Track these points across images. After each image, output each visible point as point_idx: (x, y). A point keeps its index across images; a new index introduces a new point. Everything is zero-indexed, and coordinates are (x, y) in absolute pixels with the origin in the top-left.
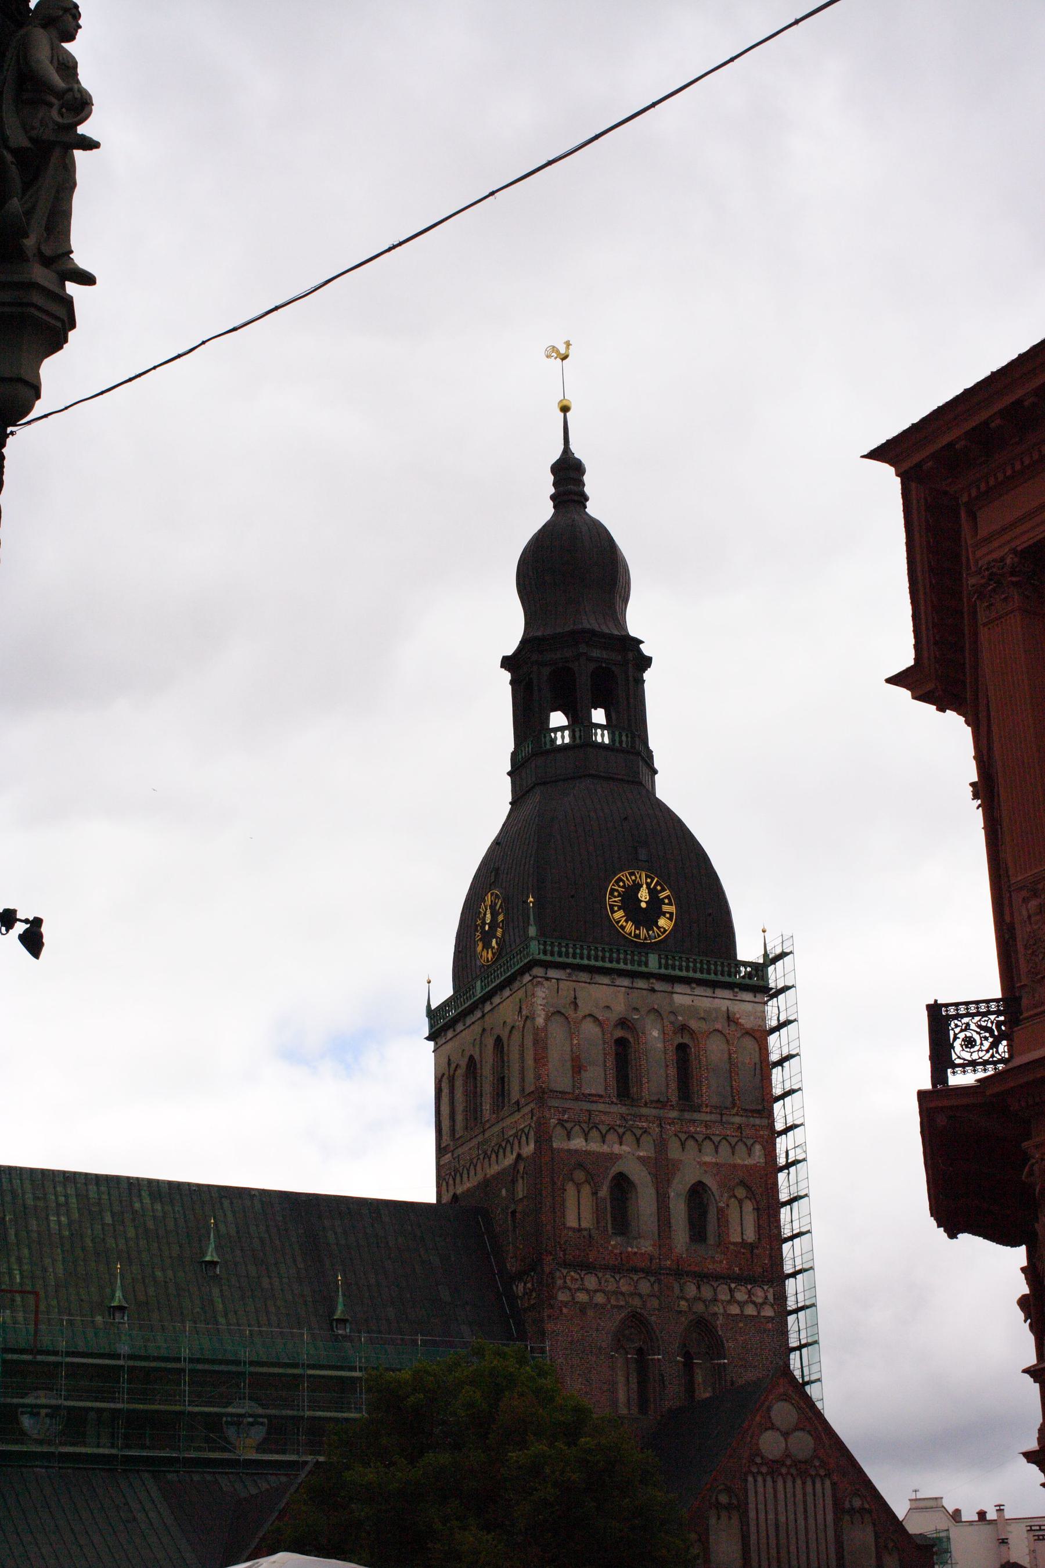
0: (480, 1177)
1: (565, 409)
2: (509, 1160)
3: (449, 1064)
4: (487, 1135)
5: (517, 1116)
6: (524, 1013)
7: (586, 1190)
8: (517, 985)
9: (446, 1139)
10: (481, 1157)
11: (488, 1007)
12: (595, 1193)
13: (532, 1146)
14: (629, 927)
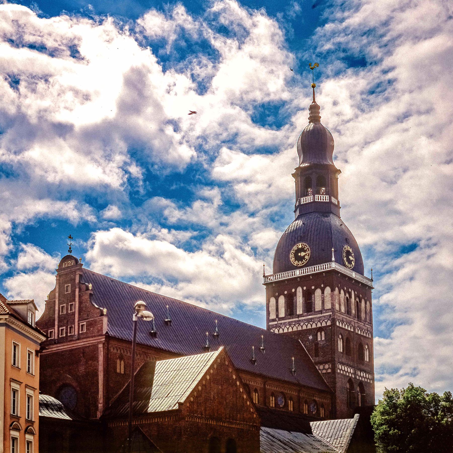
5: (320, 315)
7: (341, 340)
9: (273, 316)
10: (297, 325)
12: (343, 342)
14: (347, 263)
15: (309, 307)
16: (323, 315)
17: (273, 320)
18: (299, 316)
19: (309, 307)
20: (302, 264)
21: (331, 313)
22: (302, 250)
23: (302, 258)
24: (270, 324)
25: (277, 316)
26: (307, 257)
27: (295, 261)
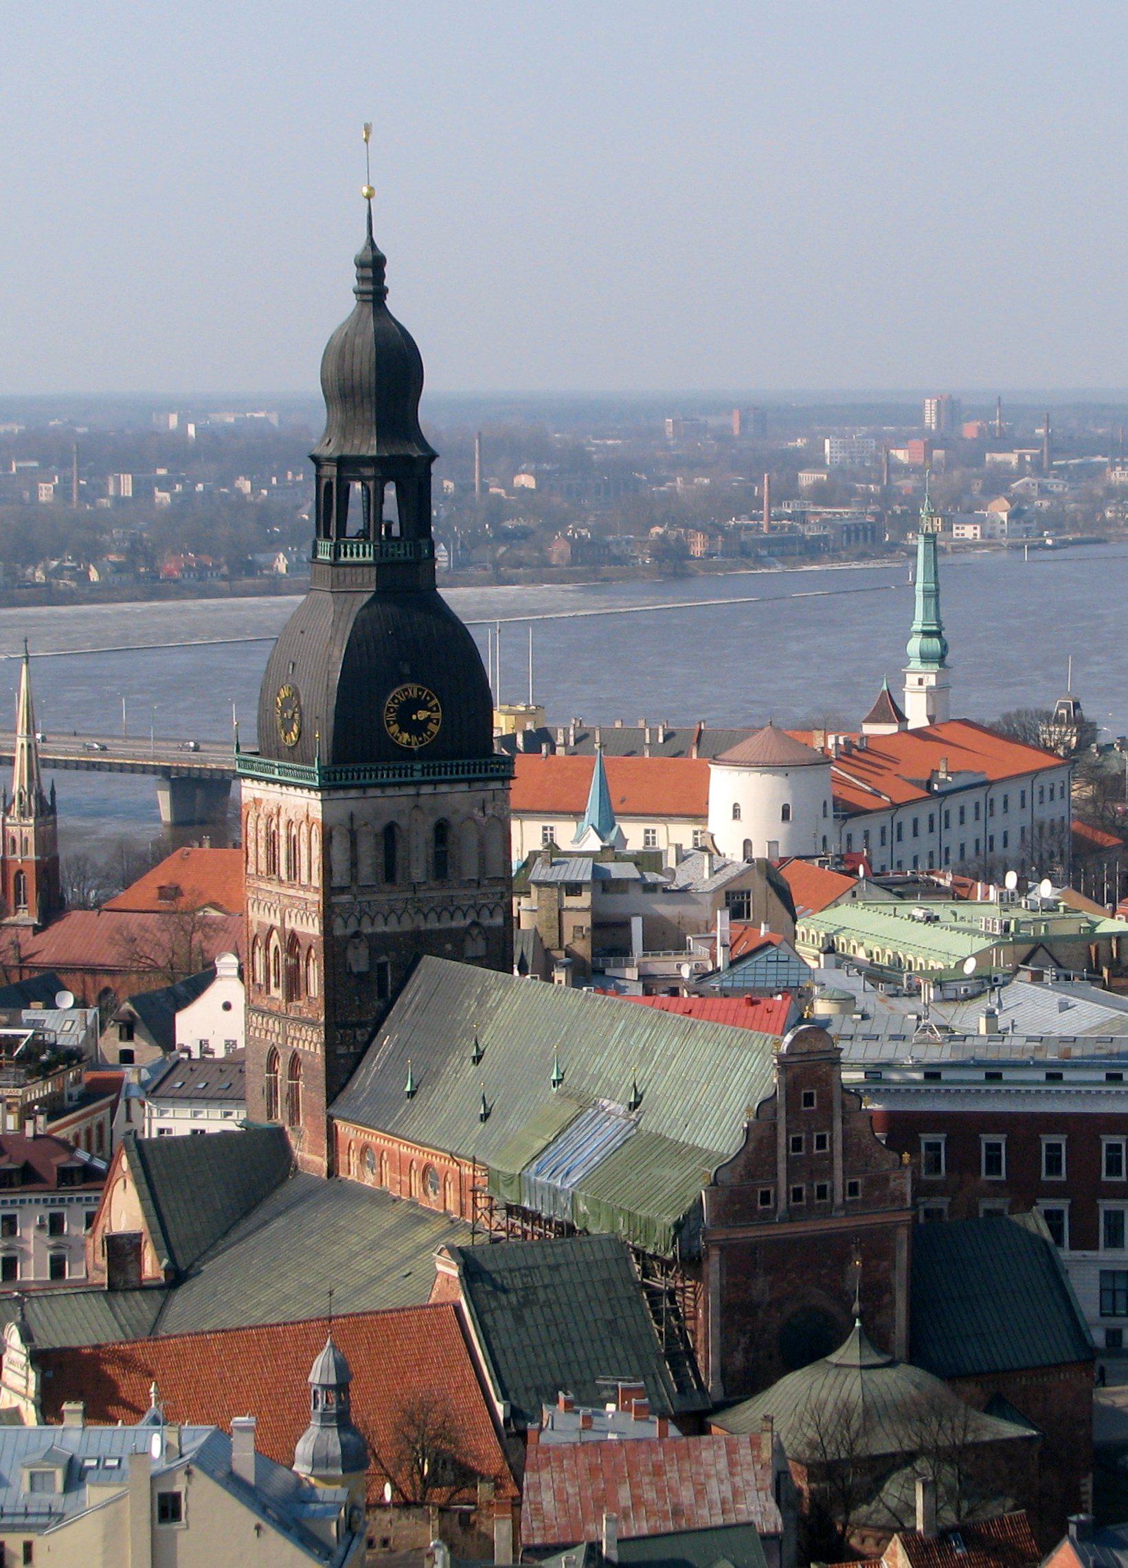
0: (407, 925)
1: (369, 197)
2: (460, 922)
3: (352, 817)
4: (420, 895)
5: (475, 892)
6: (489, 811)
8: (478, 785)
11: (426, 789)
13: (499, 920)
15: (441, 865)
16: (483, 890)
17: (342, 890)
18: (414, 887)
19: (441, 865)
20: (421, 742)
21: (504, 890)
22: (421, 704)
23: (418, 728)
24: (334, 899)
25: (354, 878)
26: (434, 728)
27: (400, 732)
